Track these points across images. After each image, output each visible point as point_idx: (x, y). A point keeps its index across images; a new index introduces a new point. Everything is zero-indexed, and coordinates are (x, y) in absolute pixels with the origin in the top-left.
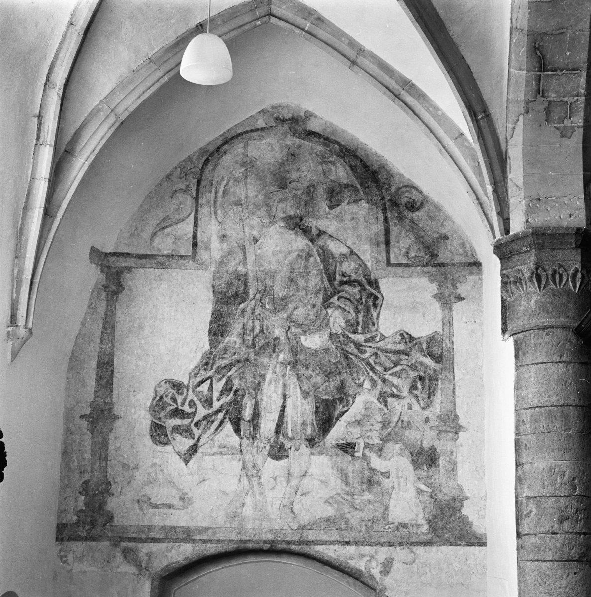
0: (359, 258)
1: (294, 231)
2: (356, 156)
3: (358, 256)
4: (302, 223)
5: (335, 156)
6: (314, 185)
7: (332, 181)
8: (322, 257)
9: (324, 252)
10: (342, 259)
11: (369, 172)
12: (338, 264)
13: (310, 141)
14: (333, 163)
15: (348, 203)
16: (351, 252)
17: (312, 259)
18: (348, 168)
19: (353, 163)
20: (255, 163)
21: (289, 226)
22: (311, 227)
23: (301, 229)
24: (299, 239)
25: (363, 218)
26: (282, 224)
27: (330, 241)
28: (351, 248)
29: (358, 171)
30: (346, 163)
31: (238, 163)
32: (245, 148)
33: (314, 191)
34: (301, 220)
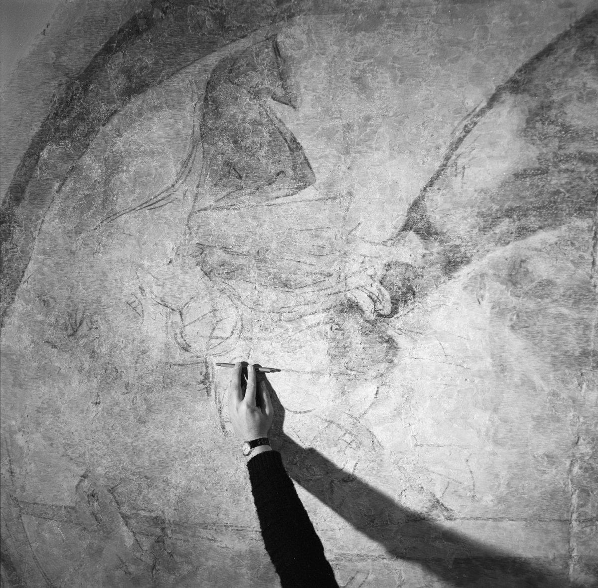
0: (549, 50)
1: (401, 341)
2: (89, 74)
3: (538, 58)
4: (367, 305)
5: (87, 160)
6: (202, 248)
7: (186, 167)
8: (532, 221)
9: (509, 213)
10: (552, 129)
11: (157, 14)
12: (572, 148)
13: (25, 258)
14: (113, 166)
15: (288, 101)
16: (515, 86)
17: (542, 268)
18: (136, 103)
19: (118, 84)
20: (102, 482)
21: (374, 361)
22: (389, 266)
23: (395, 311)
24: (438, 321)
25: (360, 35)
26: (366, 391)
27: (457, 182)
28: (500, 90)
29: (149, 62)
30: (114, 113)
31: (100, 551)
32: (42, 516)
33: (225, 249)
34: (353, 307)
